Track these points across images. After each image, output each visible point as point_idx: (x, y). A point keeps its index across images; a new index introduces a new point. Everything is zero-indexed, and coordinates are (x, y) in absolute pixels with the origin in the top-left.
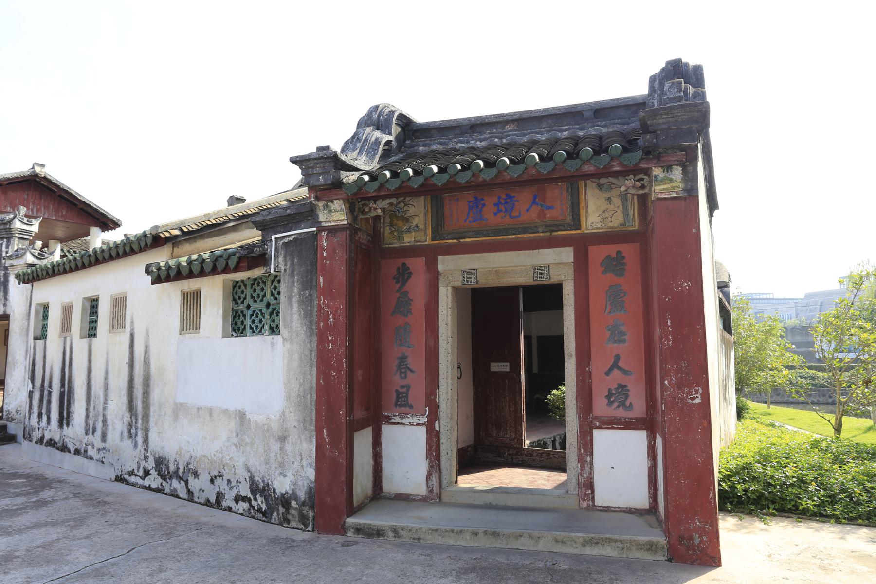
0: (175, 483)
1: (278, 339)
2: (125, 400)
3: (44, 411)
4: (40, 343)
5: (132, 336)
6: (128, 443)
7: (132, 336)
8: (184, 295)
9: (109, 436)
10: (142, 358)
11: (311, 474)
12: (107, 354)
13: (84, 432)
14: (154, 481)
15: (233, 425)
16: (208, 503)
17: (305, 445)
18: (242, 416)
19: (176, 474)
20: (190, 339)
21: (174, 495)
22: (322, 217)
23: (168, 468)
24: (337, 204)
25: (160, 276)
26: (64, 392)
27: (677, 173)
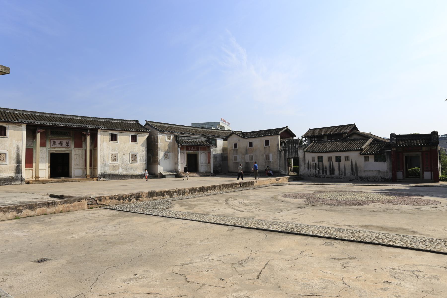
0: (365, 180)
1: (386, 162)
2: (350, 170)
3: (324, 173)
4: (320, 163)
5: (352, 162)
6: (352, 176)
7: (352, 162)
8: (364, 157)
9: (347, 175)
10: (355, 164)
11: (392, 176)
12: (345, 164)
13: (338, 175)
14: (359, 180)
15: (377, 172)
16: (372, 181)
17: (391, 173)
18: (379, 171)
19: (365, 179)
20: (367, 162)
21: (365, 181)
22: (392, 149)
23: (363, 178)
24: (395, 148)
25: (361, 154)
26: (331, 170)
27: (435, 147)
